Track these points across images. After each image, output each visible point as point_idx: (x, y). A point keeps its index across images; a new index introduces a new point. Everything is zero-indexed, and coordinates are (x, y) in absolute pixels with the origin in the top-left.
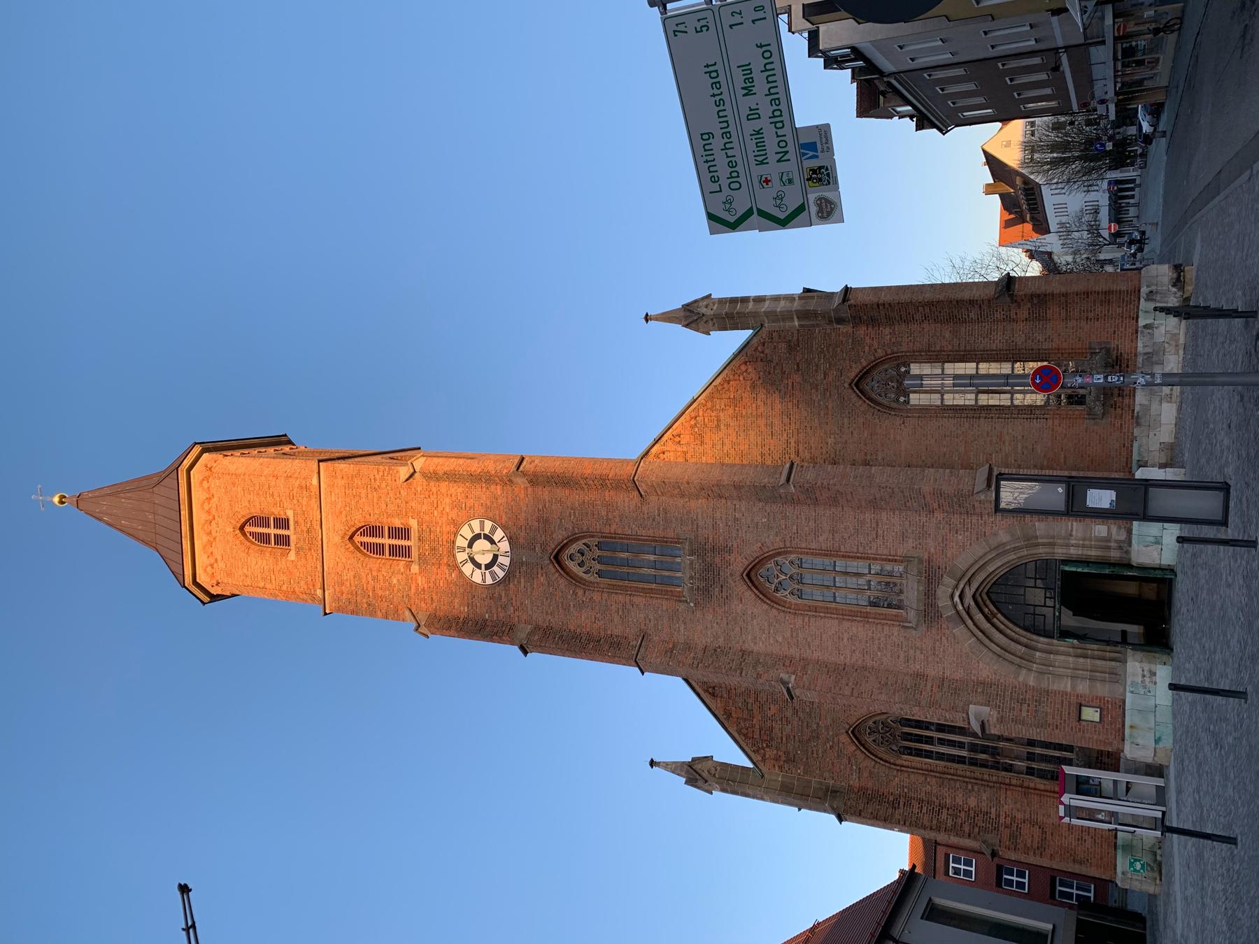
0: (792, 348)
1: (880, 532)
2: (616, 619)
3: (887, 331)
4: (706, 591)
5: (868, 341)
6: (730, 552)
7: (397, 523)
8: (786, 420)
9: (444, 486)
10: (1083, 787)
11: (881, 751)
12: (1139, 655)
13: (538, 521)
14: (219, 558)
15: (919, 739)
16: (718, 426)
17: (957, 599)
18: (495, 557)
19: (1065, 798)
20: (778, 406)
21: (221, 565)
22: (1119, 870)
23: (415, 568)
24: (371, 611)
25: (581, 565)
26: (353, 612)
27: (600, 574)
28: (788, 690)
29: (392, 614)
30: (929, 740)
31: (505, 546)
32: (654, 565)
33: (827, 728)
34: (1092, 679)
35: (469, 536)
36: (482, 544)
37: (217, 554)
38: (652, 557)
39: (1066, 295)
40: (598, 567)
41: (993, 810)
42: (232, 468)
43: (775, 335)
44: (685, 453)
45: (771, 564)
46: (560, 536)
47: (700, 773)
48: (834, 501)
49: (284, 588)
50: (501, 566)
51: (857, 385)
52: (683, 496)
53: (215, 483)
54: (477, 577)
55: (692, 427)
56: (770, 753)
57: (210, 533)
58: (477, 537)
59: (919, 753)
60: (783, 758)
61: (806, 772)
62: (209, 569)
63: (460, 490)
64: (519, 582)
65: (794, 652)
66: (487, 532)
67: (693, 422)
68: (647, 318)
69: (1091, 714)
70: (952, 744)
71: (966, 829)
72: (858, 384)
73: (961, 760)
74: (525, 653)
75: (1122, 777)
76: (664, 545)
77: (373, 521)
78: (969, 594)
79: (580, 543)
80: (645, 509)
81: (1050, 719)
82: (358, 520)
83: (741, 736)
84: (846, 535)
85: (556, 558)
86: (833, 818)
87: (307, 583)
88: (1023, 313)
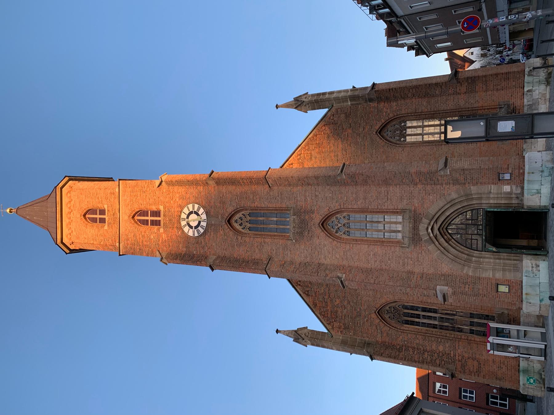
0: (347, 116)
1: (389, 197)
2: (257, 251)
3: (395, 104)
4: (301, 234)
5: (385, 110)
6: (313, 213)
7: (154, 208)
8: (344, 153)
9: (176, 188)
10: (499, 333)
11: (393, 322)
12: (530, 257)
13: (220, 203)
15: (413, 316)
16: (311, 158)
17: (430, 230)
18: (200, 222)
19: (491, 339)
20: (341, 146)
21: (74, 233)
22: (521, 383)
23: (162, 230)
24: (141, 252)
25: (241, 225)
26: (132, 254)
27: (250, 229)
28: (341, 282)
29: (151, 254)
30: (418, 316)
31: (204, 217)
32: (277, 223)
33: (365, 310)
34: (504, 270)
35: (187, 212)
36: (193, 216)
37: (75, 231)
38: (275, 219)
39: (485, 76)
40: (249, 225)
41: (452, 352)
42: (81, 187)
45: (334, 219)
46: (230, 209)
47: (301, 336)
48: (365, 182)
49: (102, 243)
50: (202, 227)
51: (380, 133)
52: (290, 185)
53: (73, 193)
54: (191, 233)
55: (298, 159)
56: (336, 324)
57: (70, 218)
58: (191, 213)
59: (412, 323)
60: (343, 327)
61: (354, 335)
62: (69, 236)
63: (183, 190)
64: (210, 234)
65: (345, 263)
66: (196, 210)
67: (299, 157)
68: (277, 107)
69: (503, 289)
70: (430, 318)
71: (438, 362)
72: (380, 132)
73: (435, 326)
74: (213, 270)
75: (522, 328)
76: (281, 212)
77: (143, 207)
78: (436, 228)
80: (271, 193)
81: (481, 292)
82: (136, 208)
83: (322, 316)
84: (372, 200)
85: (229, 221)
86: (368, 358)
87: (112, 241)
88: (463, 89)
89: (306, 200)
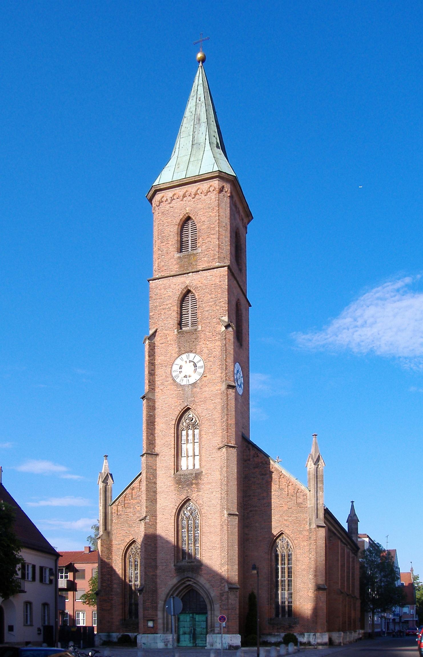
1: (211, 550)
35: (195, 361)
43: (305, 497)
44: (249, 460)
63: (217, 353)
67: (264, 462)
84: (209, 538)
87: (163, 266)
89: (209, 483)
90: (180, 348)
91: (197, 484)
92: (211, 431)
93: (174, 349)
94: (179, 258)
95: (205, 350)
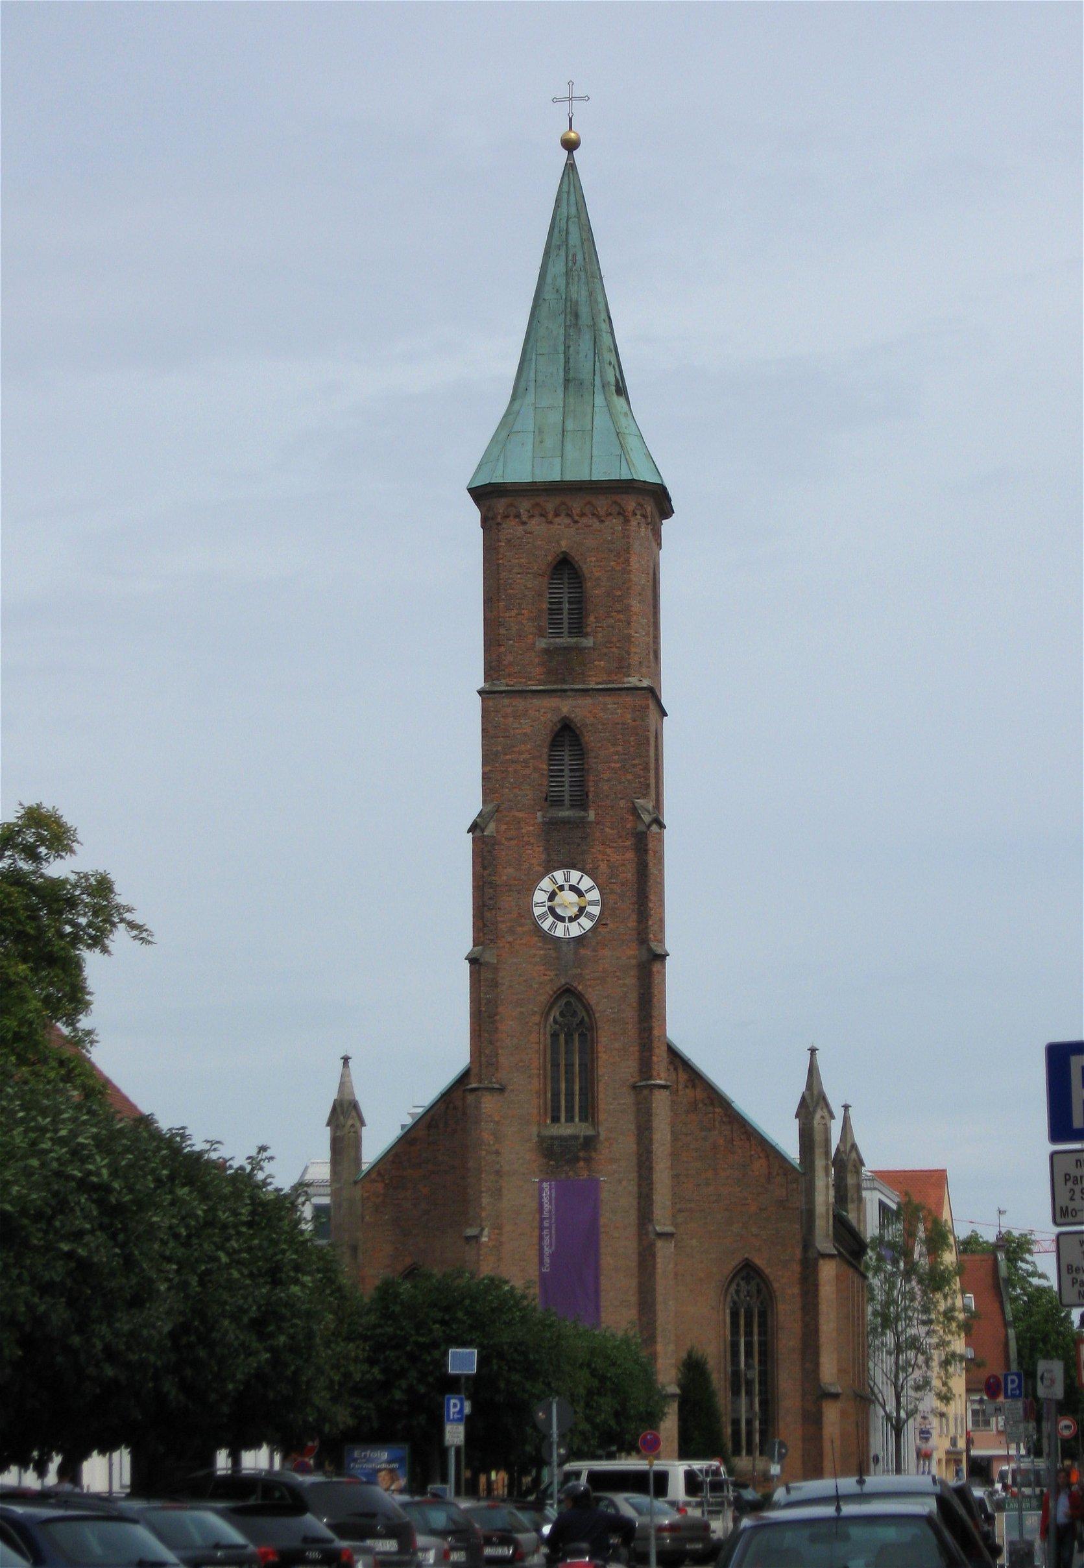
9: (630, 855)
14: (528, 527)
31: (575, 930)
54: (540, 896)
63: (629, 876)
79: (584, 1014)
87: (511, 664)
90: (549, 855)
91: (588, 1160)
92: (617, 1045)
93: (535, 854)
94: (546, 651)
95: (603, 866)
